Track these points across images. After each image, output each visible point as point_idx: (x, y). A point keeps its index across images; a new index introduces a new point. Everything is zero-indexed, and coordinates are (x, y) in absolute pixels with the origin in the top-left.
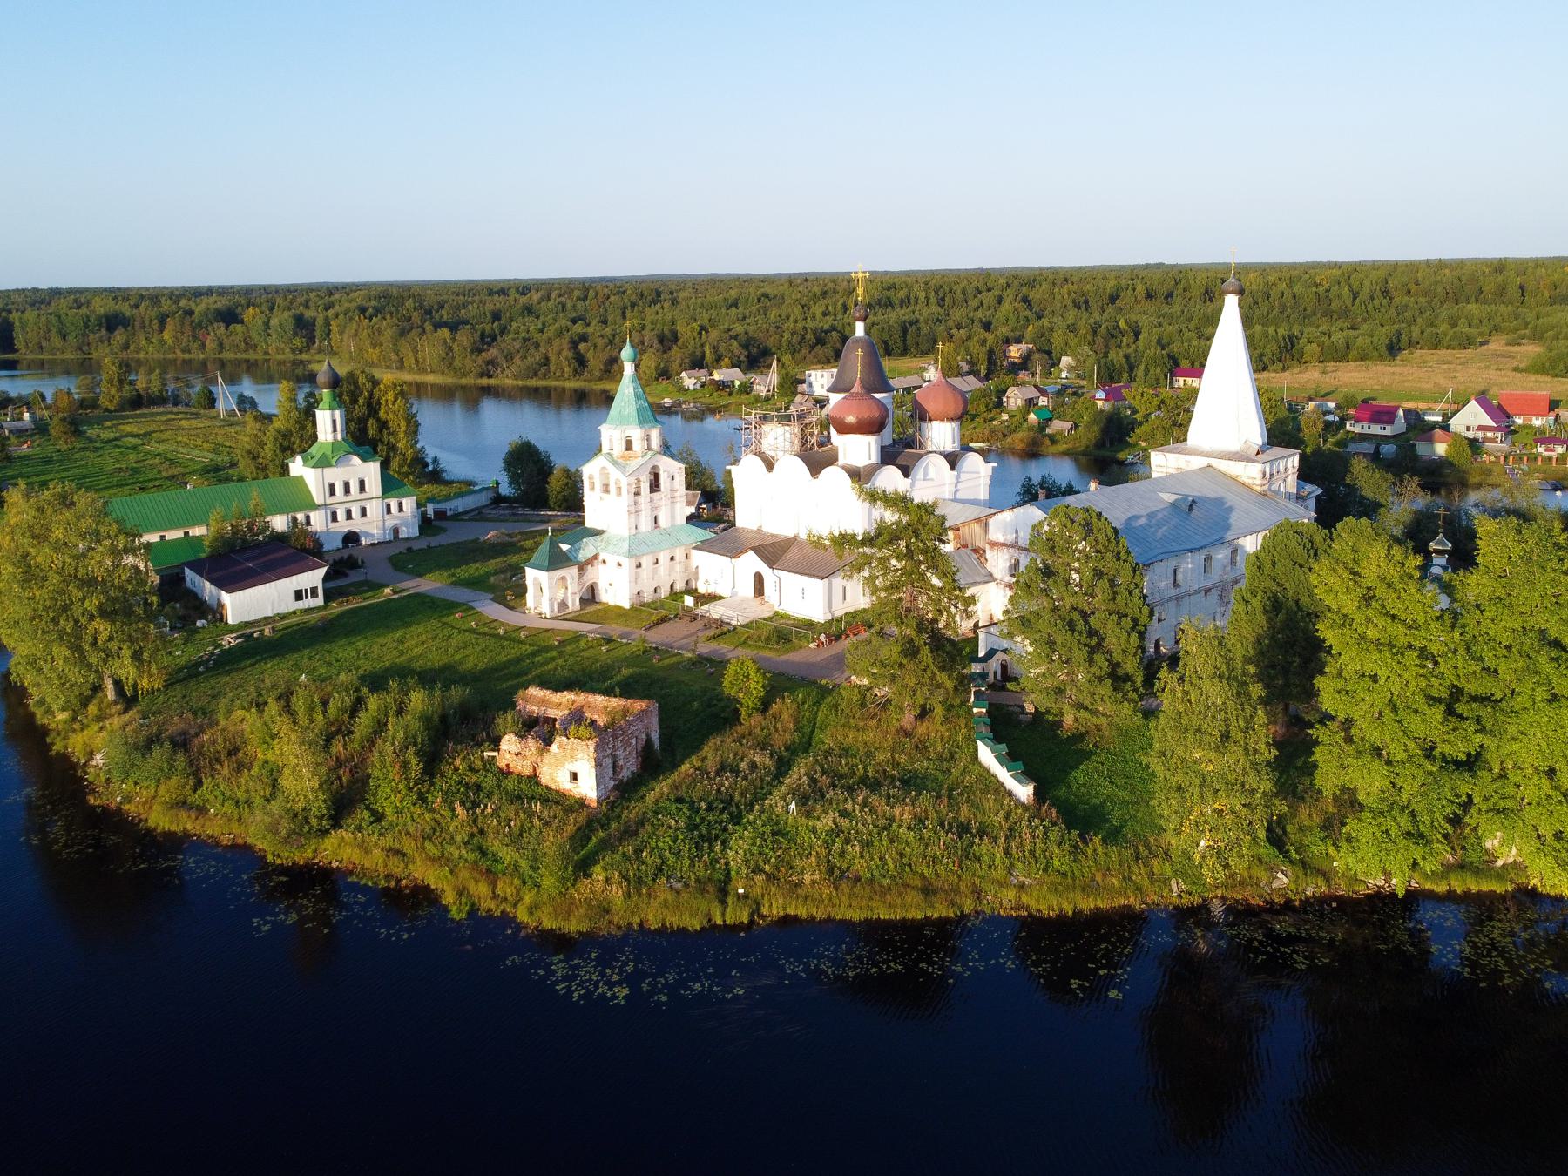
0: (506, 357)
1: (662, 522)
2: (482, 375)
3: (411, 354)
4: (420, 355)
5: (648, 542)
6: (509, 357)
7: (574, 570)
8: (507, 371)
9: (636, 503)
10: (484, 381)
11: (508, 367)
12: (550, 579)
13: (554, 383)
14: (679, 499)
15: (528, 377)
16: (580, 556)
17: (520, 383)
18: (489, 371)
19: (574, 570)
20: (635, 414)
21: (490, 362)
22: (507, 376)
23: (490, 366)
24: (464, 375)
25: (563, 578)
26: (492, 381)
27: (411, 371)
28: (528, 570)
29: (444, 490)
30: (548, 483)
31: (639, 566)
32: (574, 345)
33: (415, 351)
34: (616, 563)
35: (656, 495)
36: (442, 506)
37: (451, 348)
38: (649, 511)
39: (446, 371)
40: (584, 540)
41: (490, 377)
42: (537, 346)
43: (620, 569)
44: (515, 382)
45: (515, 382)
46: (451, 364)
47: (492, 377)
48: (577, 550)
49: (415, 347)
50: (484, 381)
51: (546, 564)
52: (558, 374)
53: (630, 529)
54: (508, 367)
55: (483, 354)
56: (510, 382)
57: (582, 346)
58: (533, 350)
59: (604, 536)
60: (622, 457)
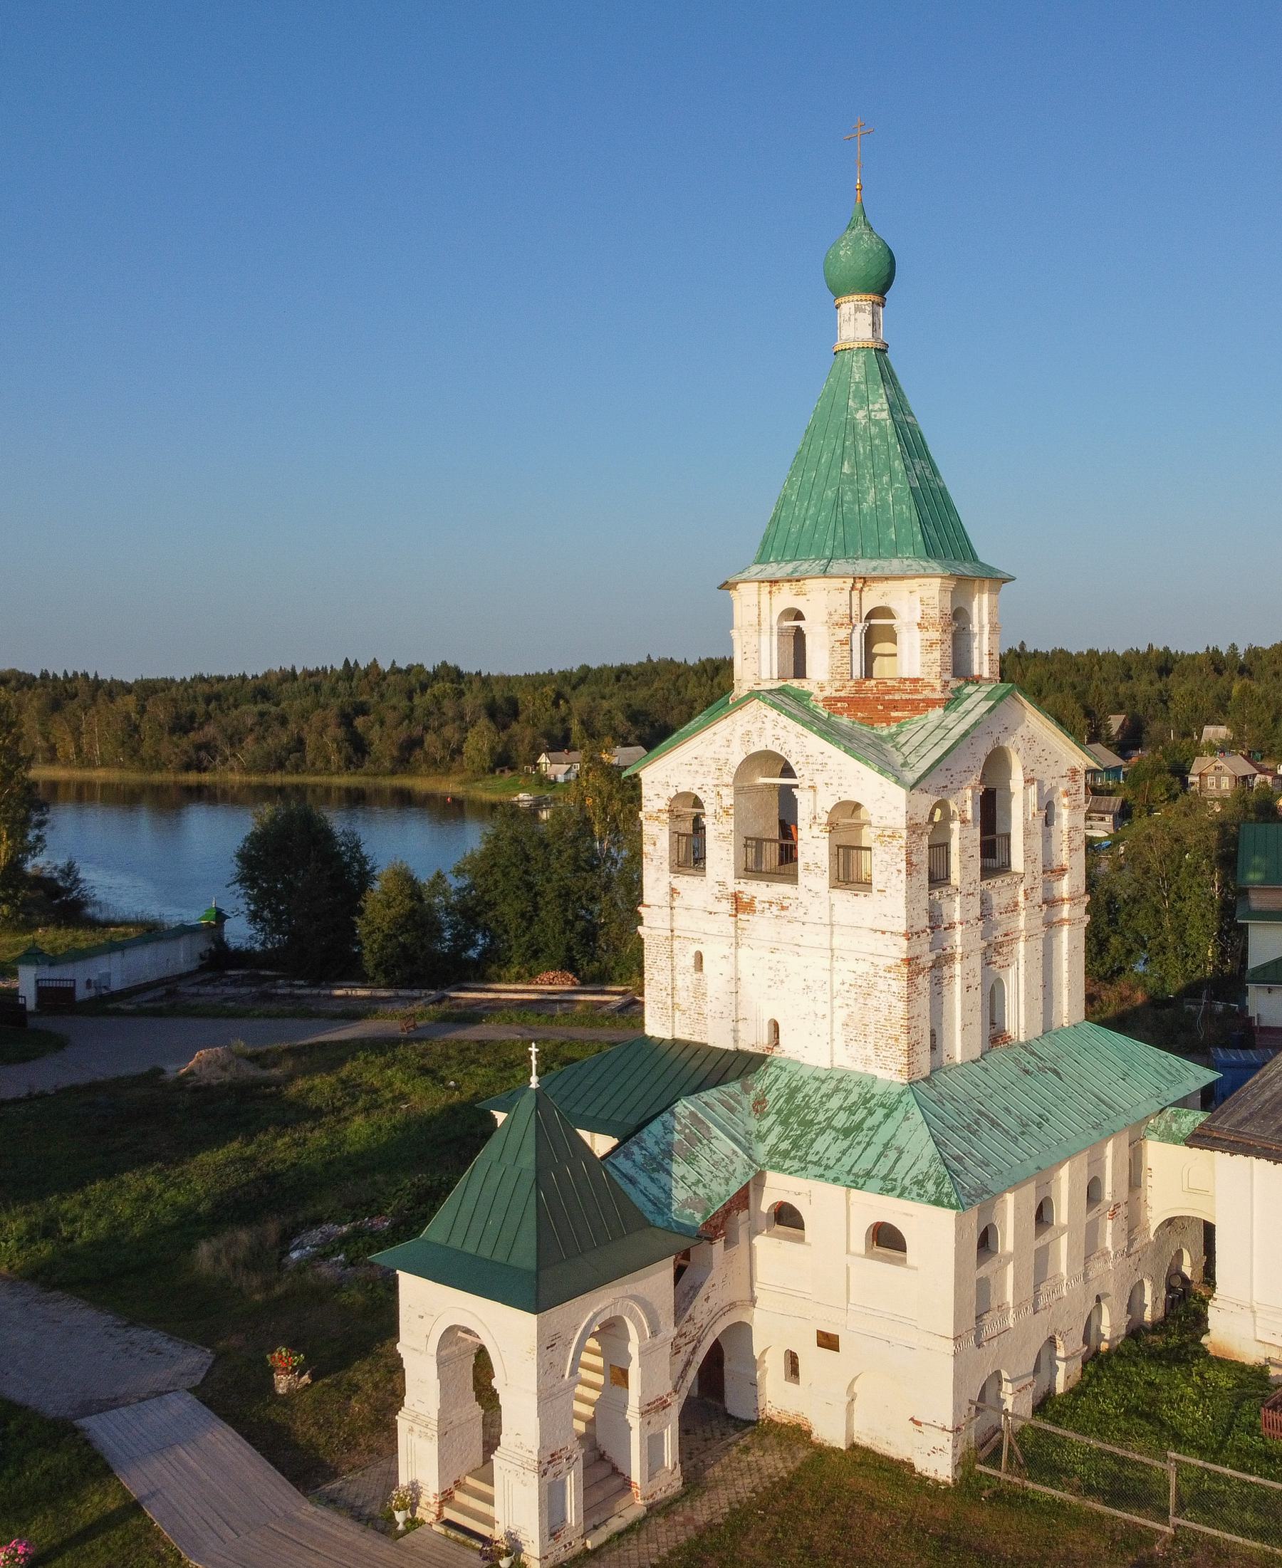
0: (231, 738)
1: (1018, 1021)
2: (187, 767)
3: (68, 738)
4: (85, 740)
5: (994, 1108)
6: (235, 739)
7: (658, 1280)
8: (232, 762)
9: (936, 923)
10: (192, 778)
11: (234, 755)
12: (549, 1344)
13: (311, 779)
14: (1065, 911)
15: (266, 770)
16: (680, 1194)
17: (255, 779)
18: (201, 762)
19: (658, 1280)
20: (907, 510)
21: (199, 747)
22: (232, 769)
23: (203, 754)
24: (159, 767)
25: (611, 1331)
26: (206, 778)
27: (68, 764)
28: (412, 1289)
29: (84, 938)
30: (361, 912)
31: (986, 1242)
32: (346, 719)
33: (77, 733)
34: (859, 1241)
35: (1000, 892)
36: (58, 974)
37: (136, 728)
38: (976, 962)
39: (128, 763)
40: (684, 1107)
41: (201, 769)
42: (283, 721)
43: (880, 1271)
44: (245, 779)
45: (245, 779)
46: (136, 751)
47: (205, 770)
48: (659, 1165)
49: (77, 729)
50: (192, 778)
51: (525, 1255)
52: (319, 765)
53: (911, 1049)
54: (234, 755)
55: (192, 734)
56: (236, 778)
57: (359, 722)
58: (276, 727)
59: (761, 1082)
60: (855, 703)
